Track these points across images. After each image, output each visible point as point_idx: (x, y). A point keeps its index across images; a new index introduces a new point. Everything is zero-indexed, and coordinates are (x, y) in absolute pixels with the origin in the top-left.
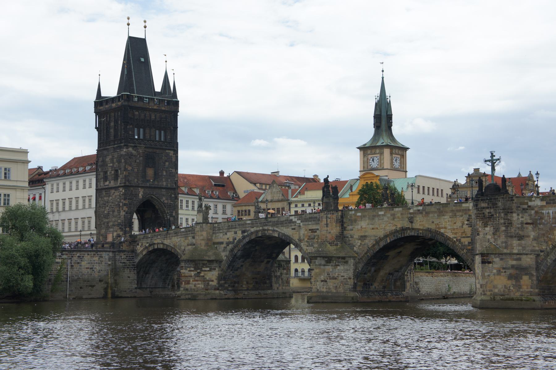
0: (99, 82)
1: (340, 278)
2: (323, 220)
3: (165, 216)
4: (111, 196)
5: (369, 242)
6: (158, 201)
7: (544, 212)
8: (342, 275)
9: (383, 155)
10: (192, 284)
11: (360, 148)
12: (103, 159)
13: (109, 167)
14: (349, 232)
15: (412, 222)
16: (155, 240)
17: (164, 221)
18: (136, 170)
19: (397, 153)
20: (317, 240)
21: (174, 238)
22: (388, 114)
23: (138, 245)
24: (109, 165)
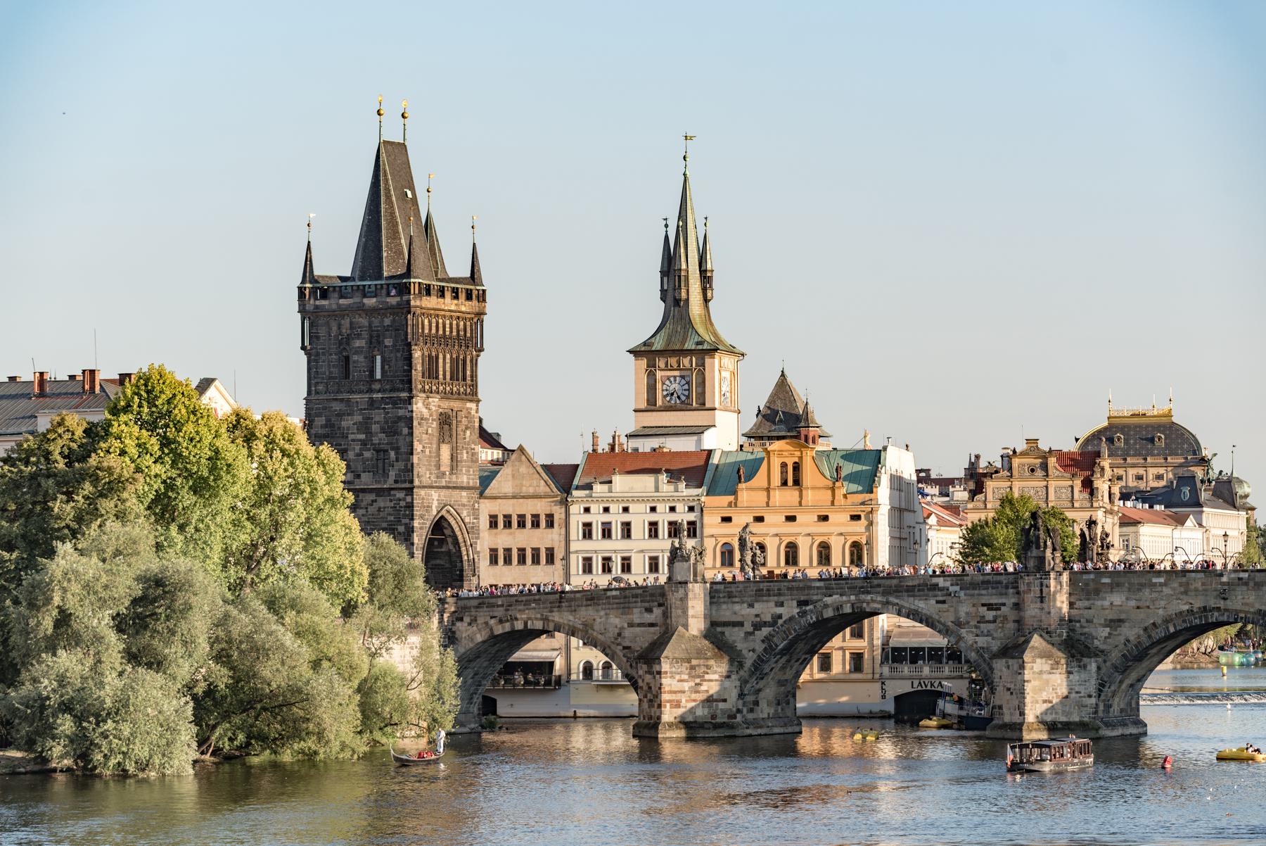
0: (309, 242)
3: (464, 553)
4: (362, 508)
5: (1130, 632)
8: (1077, 690)
11: (635, 352)
12: (328, 420)
13: (353, 440)
14: (1081, 612)
15: (1225, 599)
16: (520, 610)
17: (459, 565)
18: (427, 450)
19: (726, 366)
20: (1000, 625)
21: (584, 608)
23: (461, 619)
24: (351, 437)
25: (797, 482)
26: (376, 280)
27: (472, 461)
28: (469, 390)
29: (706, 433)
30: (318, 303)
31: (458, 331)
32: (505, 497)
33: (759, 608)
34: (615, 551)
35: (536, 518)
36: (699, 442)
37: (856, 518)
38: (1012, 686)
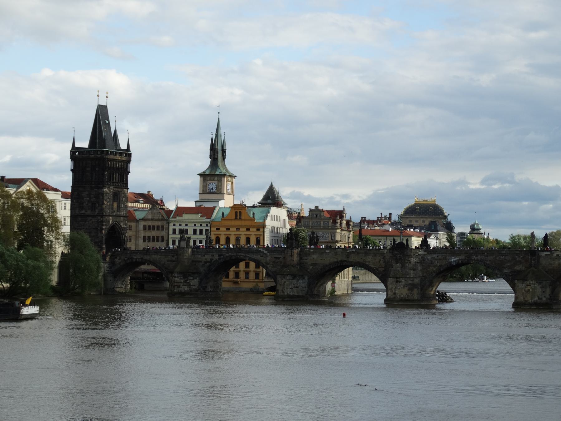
1: (300, 287)
2: (289, 253)
3: (122, 237)
6: (118, 226)
7: (426, 257)
8: (301, 285)
9: (221, 182)
10: (182, 287)
15: (348, 258)
16: (134, 256)
18: (109, 204)
19: (229, 180)
21: (153, 255)
22: (223, 148)
23: (116, 258)
24: (85, 199)
25: (240, 219)
26: (95, 149)
27: (125, 207)
28: (125, 185)
29: (220, 202)
30: (76, 156)
31: (121, 166)
32: (149, 220)
33: (206, 256)
34: (177, 238)
35: (158, 227)
36: (218, 204)
37: (258, 230)
38: (281, 283)
